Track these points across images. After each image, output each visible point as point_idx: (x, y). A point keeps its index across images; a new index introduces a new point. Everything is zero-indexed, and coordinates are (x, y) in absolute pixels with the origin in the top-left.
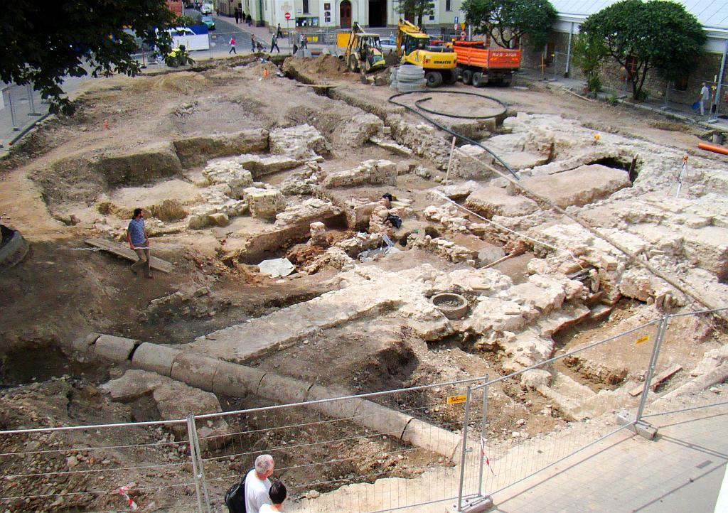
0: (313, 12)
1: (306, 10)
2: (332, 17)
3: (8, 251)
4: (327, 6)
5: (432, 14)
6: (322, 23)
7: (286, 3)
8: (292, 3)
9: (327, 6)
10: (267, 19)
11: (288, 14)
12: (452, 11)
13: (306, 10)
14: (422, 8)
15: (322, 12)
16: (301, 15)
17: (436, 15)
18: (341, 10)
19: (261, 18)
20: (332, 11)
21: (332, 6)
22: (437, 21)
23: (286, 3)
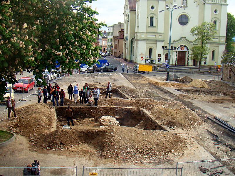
0: (153, 58)
1: (150, 57)
2: (161, 60)
3: (1, 151)
4: (160, 56)
5: (205, 61)
6: (157, 62)
7: (142, 53)
8: (144, 53)
9: (160, 56)
10: (134, 59)
11: (142, 57)
12: (214, 60)
13: (150, 57)
14: (201, 58)
15: (157, 58)
16: (148, 58)
17: (207, 61)
18: (165, 57)
19: (131, 59)
20: (161, 58)
21: (162, 56)
22: (207, 64)
23: (142, 53)
